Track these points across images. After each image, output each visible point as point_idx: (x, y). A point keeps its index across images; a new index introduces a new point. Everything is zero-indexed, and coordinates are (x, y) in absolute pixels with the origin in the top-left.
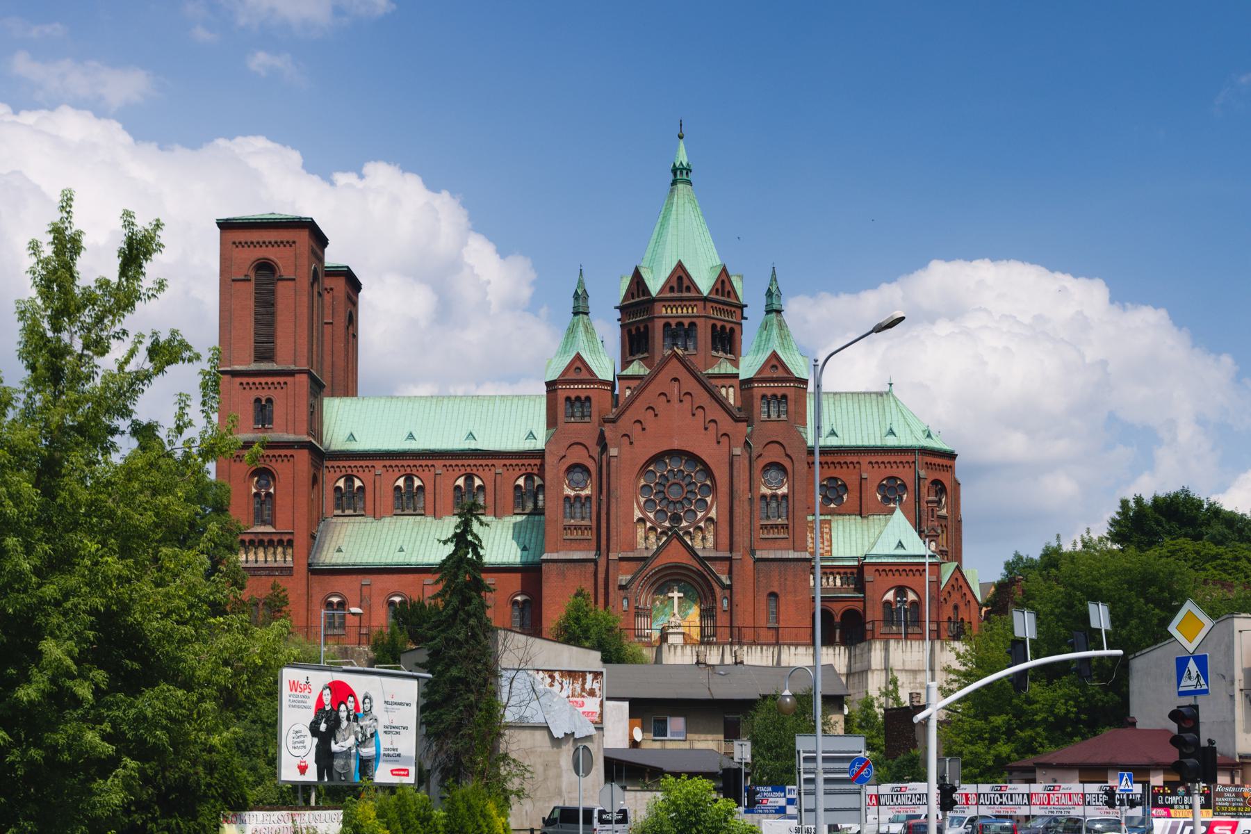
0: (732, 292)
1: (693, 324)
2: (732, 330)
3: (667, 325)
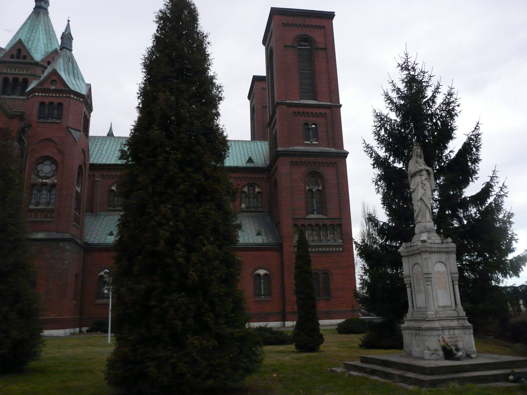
3: (6, 80)
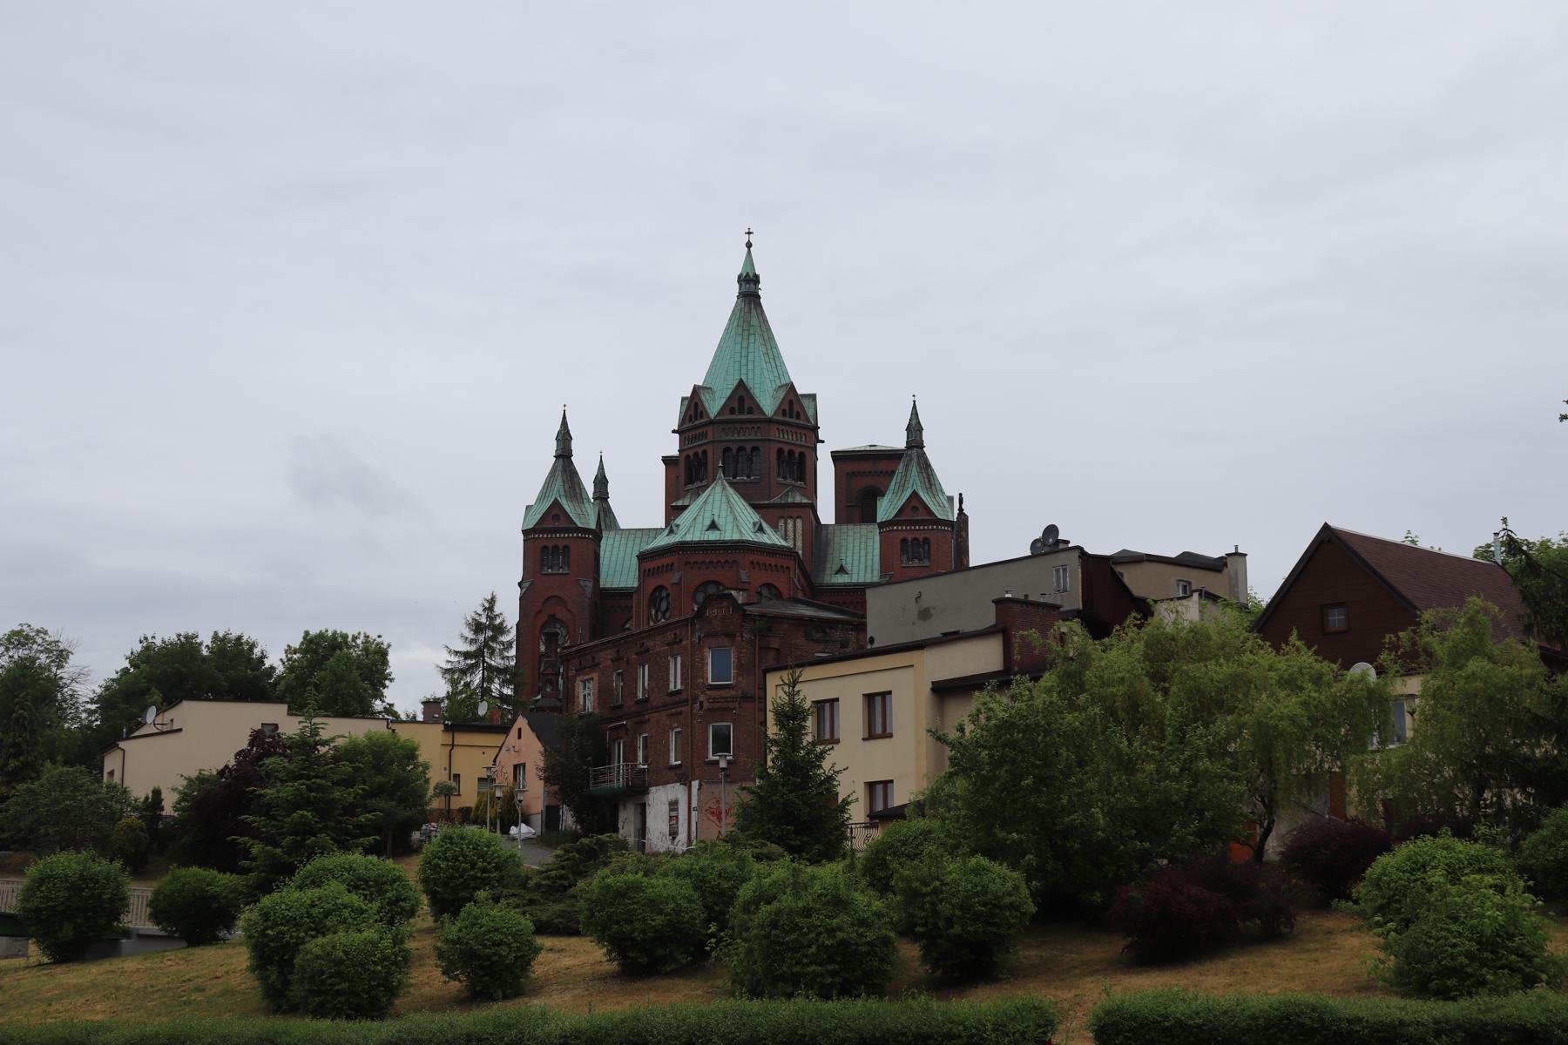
0: (802, 414)
2: (802, 455)
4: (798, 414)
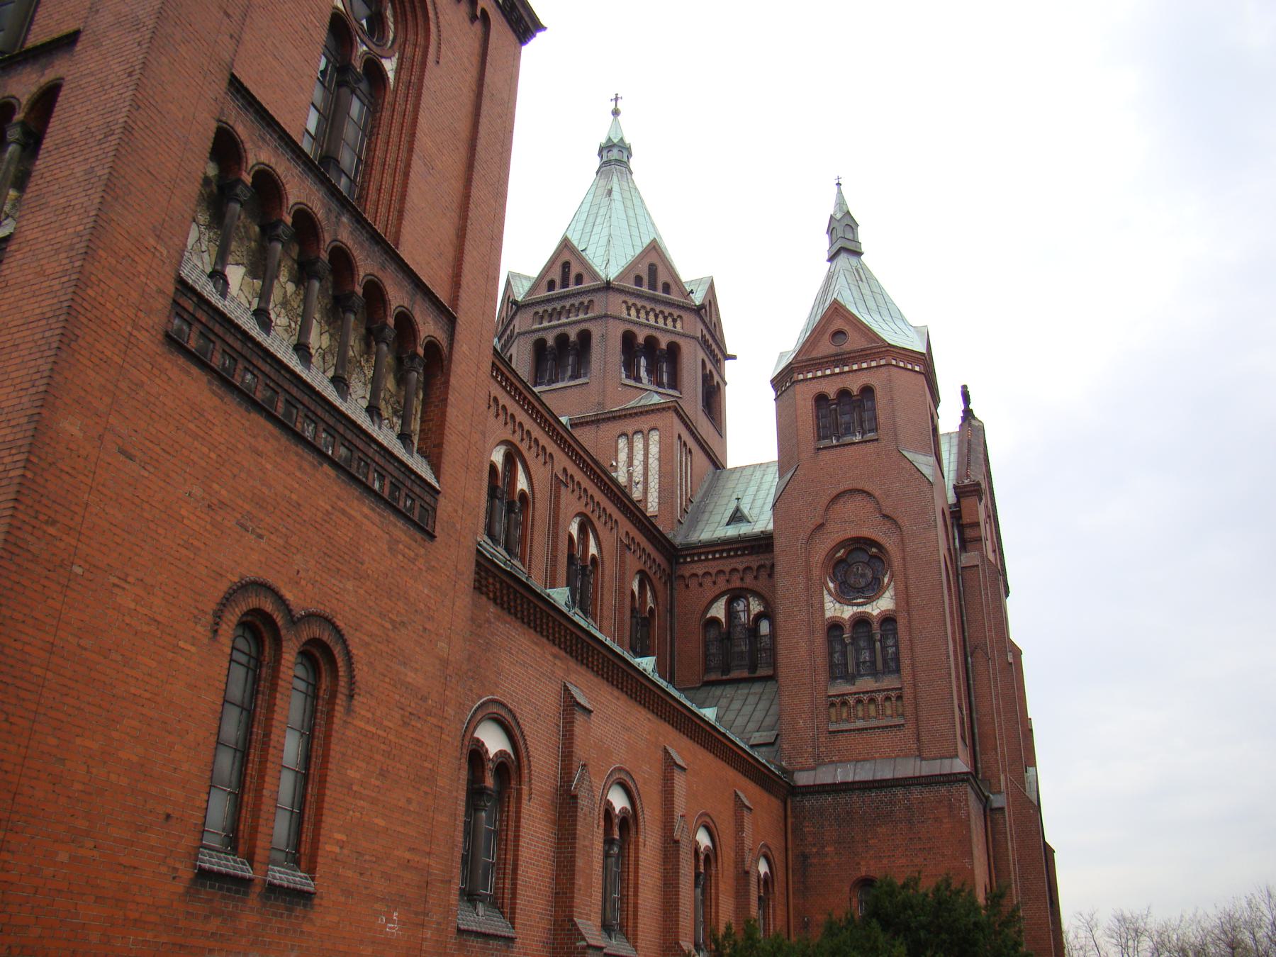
1: (585, 337)
3: (540, 346)
4: (667, 288)
